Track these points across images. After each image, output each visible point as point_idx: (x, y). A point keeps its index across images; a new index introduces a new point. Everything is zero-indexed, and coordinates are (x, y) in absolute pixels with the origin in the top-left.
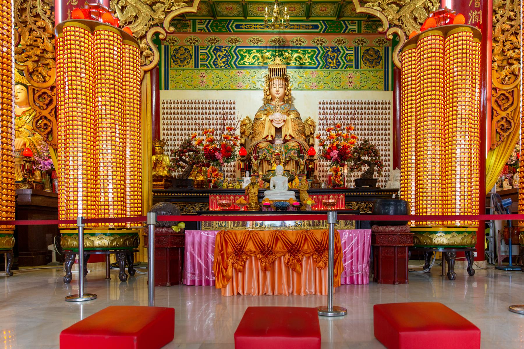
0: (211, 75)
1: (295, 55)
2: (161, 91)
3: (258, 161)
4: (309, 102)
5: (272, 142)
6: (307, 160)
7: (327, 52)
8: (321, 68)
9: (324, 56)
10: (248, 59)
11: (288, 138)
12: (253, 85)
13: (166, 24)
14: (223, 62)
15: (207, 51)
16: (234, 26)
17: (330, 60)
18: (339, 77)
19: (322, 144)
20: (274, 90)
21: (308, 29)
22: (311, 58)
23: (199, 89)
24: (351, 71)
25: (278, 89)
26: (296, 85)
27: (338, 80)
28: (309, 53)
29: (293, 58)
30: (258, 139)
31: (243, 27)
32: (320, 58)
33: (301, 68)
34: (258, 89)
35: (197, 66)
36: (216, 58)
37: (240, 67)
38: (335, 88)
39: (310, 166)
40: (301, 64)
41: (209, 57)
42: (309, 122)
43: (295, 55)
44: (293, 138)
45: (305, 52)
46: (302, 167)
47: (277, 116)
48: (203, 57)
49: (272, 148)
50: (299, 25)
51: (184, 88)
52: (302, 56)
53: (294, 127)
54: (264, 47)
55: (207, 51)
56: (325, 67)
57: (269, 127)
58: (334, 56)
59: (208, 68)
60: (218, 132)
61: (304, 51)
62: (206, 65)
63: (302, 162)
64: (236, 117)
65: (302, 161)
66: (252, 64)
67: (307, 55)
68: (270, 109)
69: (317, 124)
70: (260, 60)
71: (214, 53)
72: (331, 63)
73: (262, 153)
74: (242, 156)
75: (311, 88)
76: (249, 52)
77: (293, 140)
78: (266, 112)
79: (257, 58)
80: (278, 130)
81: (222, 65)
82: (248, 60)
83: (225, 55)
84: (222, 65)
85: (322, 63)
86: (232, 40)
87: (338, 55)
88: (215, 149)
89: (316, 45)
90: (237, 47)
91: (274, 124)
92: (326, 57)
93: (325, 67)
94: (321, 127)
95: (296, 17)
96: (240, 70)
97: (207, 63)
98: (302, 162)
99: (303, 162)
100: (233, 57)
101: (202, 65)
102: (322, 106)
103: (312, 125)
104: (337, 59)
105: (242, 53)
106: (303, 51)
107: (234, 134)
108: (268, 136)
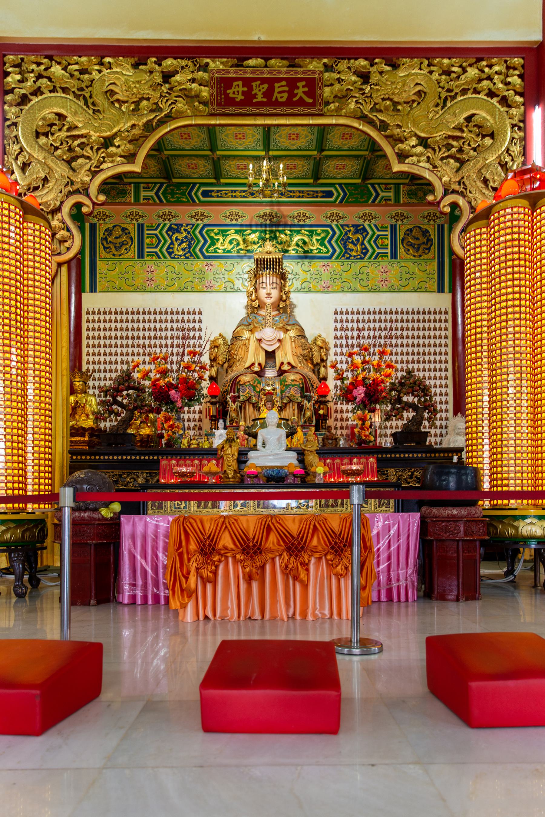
0: (162, 269)
1: (296, 238)
2: (83, 294)
3: (238, 404)
5: (260, 374)
6: (316, 402)
7: (346, 234)
8: (337, 258)
9: (342, 239)
11: (286, 367)
12: (229, 285)
14: (183, 250)
15: (157, 232)
16: (199, 194)
18: (365, 272)
19: (340, 377)
20: (263, 293)
21: (317, 197)
23: (145, 291)
24: (385, 263)
25: (269, 291)
26: (297, 284)
28: (319, 235)
29: (294, 243)
31: (213, 194)
32: (336, 242)
33: (306, 257)
34: (238, 290)
35: (141, 255)
36: (172, 243)
37: (209, 257)
38: (360, 289)
39: (321, 412)
40: (305, 252)
41: (160, 241)
43: (296, 238)
44: (293, 367)
45: (311, 234)
46: (308, 414)
47: (268, 333)
48: (152, 242)
49: (260, 383)
50: (303, 192)
52: (306, 239)
53: (295, 350)
54: (247, 226)
55: (157, 232)
56: (343, 256)
57: (256, 351)
58: (358, 240)
59: (159, 257)
60: (175, 358)
61: (311, 232)
62: (156, 253)
63: (308, 405)
64: (203, 334)
65: (308, 405)
66: (229, 251)
67: (315, 238)
68: (257, 322)
69: (331, 345)
70: (242, 246)
71: (168, 235)
72: (352, 250)
73: (243, 392)
74: (212, 397)
75: (322, 289)
76: (224, 234)
77: (294, 370)
78: (250, 327)
79: (235, 243)
80: (270, 355)
81: (181, 253)
82: (222, 245)
83: (186, 237)
84: (181, 253)
85: (338, 251)
87: (364, 238)
88: (170, 386)
89: (328, 222)
90: (205, 226)
91: (263, 345)
92: (345, 241)
93: (343, 256)
94: (339, 350)
95: (298, 178)
97: (157, 250)
98: (308, 405)
99: (310, 407)
100: (199, 241)
101: (150, 254)
103: (324, 347)
105: (212, 235)
106: (309, 231)
107: (199, 362)
108: (253, 364)
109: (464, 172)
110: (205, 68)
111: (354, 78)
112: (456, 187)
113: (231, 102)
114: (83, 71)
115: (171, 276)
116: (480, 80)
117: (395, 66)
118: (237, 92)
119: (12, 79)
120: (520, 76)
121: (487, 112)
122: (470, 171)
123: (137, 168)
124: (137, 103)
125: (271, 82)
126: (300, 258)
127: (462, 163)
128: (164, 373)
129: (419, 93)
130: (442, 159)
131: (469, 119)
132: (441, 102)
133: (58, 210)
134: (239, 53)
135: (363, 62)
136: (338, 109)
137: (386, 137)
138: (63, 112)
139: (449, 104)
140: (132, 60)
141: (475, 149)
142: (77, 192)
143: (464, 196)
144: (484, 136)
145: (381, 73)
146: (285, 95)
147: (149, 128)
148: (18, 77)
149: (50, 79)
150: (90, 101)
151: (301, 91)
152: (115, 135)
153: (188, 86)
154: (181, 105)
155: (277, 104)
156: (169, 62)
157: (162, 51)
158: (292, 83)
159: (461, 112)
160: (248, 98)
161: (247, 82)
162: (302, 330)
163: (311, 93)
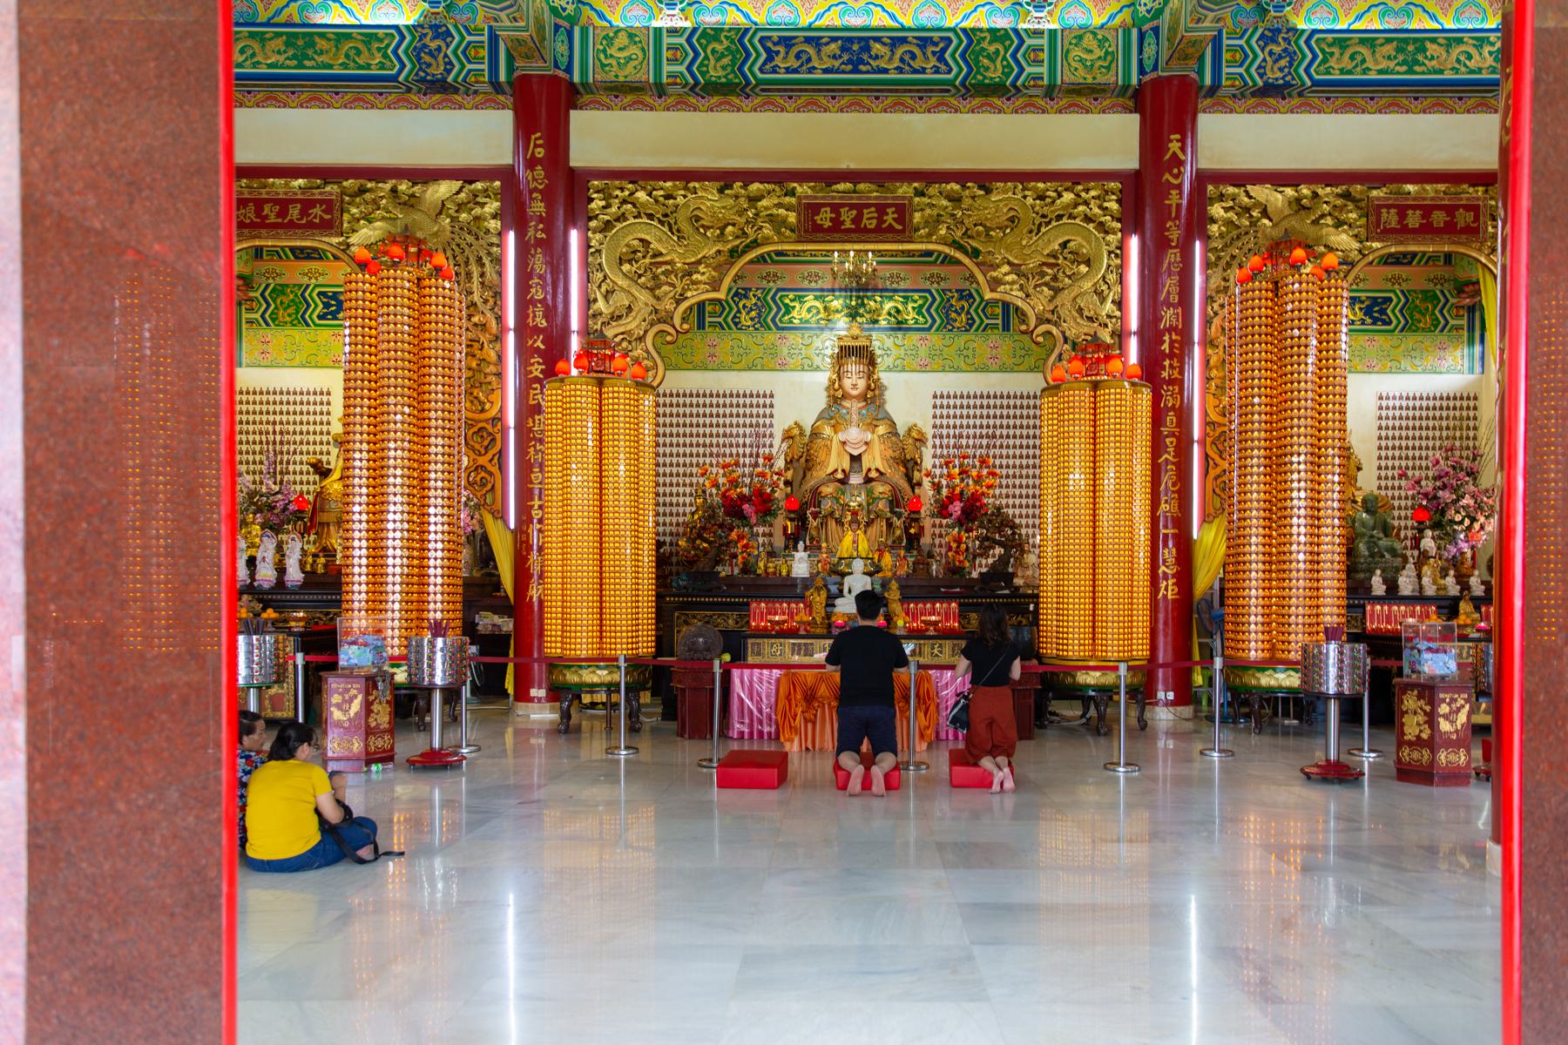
0: (727, 343)
1: (888, 305)
5: (843, 482)
11: (873, 474)
12: (806, 362)
13: (677, 321)
20: (847, 383)
22: (919, 311)
24: (995, 337)
25: (854, 380)
26: (889, 361)
27: (970, 353)
30: (819, 474)
33: (900, 329)
34: (817, 369)
35: (701, 326)
40: (899, 322)
42: (914, 434)
43: (888, 305)
47: (854, 434)
52: (900, 307)
60: (747, 460)
66: (807, 322)
67: (910, 305)
69: (930, 437)
76: (800, 299)
82: (799, 313)
86: (768, 274)
88: (743, 498)
89: (927, 285)
90: (779, 290)
92: (946, 309)
94: (938, 442)
96: (784, 333)
99: (900, 519)
101: (712, 324)
102: (938, 402)
103: (921, 440)
104: (968, 313)
109: (1058, 301)
110: (792, 193)
111: (945, 203)
112: (1049, 316)
113: (818, 228)
116: (1075, 206)
117: (988, 191)
118: (825, 218)
119: (597, 204)
121: (1084, 238)
122: (1065, 298)
123: (721, 295)
124: (723, 229)
125: (860, 208)
126: (893, 329)
127: (1057, 291)
128: (734, 483)
129: (1012, 219)
130: (1036, 286)
131: (1064, 245)
133: (641, 339)
134: (829, 178)
135: (956, 187)
136: (930, 235)
137: (977, 264)
138: (648, 238)
139: (1043, 230)
140: (718, 185)
142: (659, 322)
143: (1056, 324)
144: (1079, 263)
146: (874, 222)
147: (735, 254)
148: (603, 203)
150: (675, 228)
151: (890, 218)
152: (699, 262)
153: (775, 211)
154: (767, 230)
155: (866, 230)
156: (755, 187)
157: (748, 176)
158: (881, 209)
159: (1056, 238)
160: (837, 223)
161: (836, 208)
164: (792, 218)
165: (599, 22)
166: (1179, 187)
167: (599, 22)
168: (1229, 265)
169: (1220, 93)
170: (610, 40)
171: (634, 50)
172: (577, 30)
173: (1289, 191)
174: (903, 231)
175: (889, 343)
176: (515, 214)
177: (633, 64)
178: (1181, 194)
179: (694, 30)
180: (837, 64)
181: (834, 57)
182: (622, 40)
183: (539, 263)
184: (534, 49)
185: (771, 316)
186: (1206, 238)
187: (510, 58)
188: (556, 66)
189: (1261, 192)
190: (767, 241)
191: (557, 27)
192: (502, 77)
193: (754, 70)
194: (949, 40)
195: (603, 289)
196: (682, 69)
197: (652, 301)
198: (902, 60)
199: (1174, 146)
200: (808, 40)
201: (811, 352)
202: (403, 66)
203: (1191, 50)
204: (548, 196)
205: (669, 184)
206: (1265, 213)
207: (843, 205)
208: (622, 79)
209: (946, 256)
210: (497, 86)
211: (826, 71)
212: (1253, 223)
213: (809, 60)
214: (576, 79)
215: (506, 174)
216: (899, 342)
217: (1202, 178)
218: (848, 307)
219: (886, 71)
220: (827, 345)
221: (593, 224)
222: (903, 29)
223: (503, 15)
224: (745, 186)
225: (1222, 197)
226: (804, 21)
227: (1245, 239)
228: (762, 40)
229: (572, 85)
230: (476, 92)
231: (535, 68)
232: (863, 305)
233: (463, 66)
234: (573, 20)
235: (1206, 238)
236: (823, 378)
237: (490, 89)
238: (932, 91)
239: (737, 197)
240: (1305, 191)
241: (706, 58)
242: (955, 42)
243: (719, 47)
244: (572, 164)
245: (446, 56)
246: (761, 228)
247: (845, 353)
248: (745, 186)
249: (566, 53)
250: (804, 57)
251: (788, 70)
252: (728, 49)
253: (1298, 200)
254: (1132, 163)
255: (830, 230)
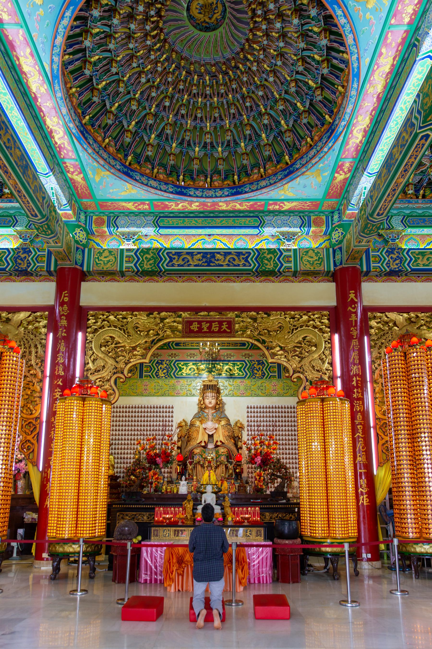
1: (226, 367)
3: (193, 465)
4: (238, 407)
10: (186, 370)
13: (126, 372)
17: (255, 371)
19: (249, 449)
22: (240, 369)
24: (275, 381)
25: (210, 400)
26: (226, 392)
27: (263, 388)
34: (194, 395)
35: (141, 376)
40: (231, 375)
43: (226, 367)
45: (234, 365)
51: (129, 395)
66: (189, 374)
67: (236, 367)
70: (196, 372)
76: (186, 365)
82: (185, 371)
86: (172, 354)
89: (243, 358)
90: (176, 361)
92: (252, 369)
96: (178, 380)
101: (146, 376)
102: (249, 410)
104: (262, 370)
109: (303, 363)
111: (249, 320)
114: (124, 318)
115: (157, 387)
117: (269, 315)
119: (91, 321)
120: (328, 319)
122: (306, 362)
123: (147, 361)
126: (228, 378)
127: (302, 358)
129: (280, 327)
130: (292, 357)
131: (304, 338)
132: (291, 331)
133: (108, 380)
134: (197, 310)
135: (254, 313)
137: (265, 347)
138: (114, 336)
139: (294, 332)
141: (307, 352)
144: (312, 346)
145: (262, 318)
149: (108, 322)
154: (169, 332)
156: (163, 314)
158: (221, 323)
159: (300, 335)
162: (228, 420)
163: (229, 327)
164: (180, 327)
165: (96, 247)
166: (356, 313)
167: (96, 247)
168: (381, 347)
169: (370, 274)
170: (100, 254)
171: (111, 258)
172: (86, 250)
173: (405, 315)
174: (231, 332)
175: (226, 384)
176: (53, 326)
177: (110, 263)
178: (357, 316)
179: (138, 249)
180: (200, 263)
181: (199, 260)
182: (106, 253)
183: (62, 347)
184: (65, 255)
185: (172, 372)
186: (369, 335)
187: (56, 261)
188: (76, 263)
189: (393, 316)
190: (168, 337)
191: (78, 249)
192: (52, 269)
193: (164, 266)
194: (250, 253)
195: (92, 358)
196: (132, 265)
197: (116, 364)
198: (229, 261)
199: (352, 296)
200: (188, 253)
201: (191, 388)
202: (9, 264)
203: (356, 255)
204: (68, 318)
205: (124, 313)
206: (395, 324)
207: (203, 321)
208: (105, 269)
209: (252, 344)
210: (50, 273)
211: (195, 266)
212: (390, 329)
213: (188, 261)
214: (85, 269)
215: (51, 309)
216: (231, 383)
217: (366, 310)
218: (208, 368)
219: (222, 266)
220: (198, 384)
221: (89, 330)
222: (229, 249)
223: (51, 241)
224: (159, 314)
225: (375, 318)
226: (187, 246)
227: (387, 335)
228: (167, 253)
229: (83, 272)
230: (41, 275)
231: (67, 264)
232: (215, 367)
233: (35, 264)
234: (85, 246)
235: (369, 335)
236: (196, 400)
237: (46, 274)
238: (242, 274)
239: (155, 318)
240: (412, 315)
241: (143, 260)
242: (252, 254)
243: (148, 256)
244: (81, 304)
245: (28, 260)
246: (166, 331)
247: (206, 388)
248: (159, 314)
249: (81, 259)
250: (186, 260)
251: (179, 265)
252: (152, 257)
253: (410, 319)
254: (333, 303)
255: (197, 332)
